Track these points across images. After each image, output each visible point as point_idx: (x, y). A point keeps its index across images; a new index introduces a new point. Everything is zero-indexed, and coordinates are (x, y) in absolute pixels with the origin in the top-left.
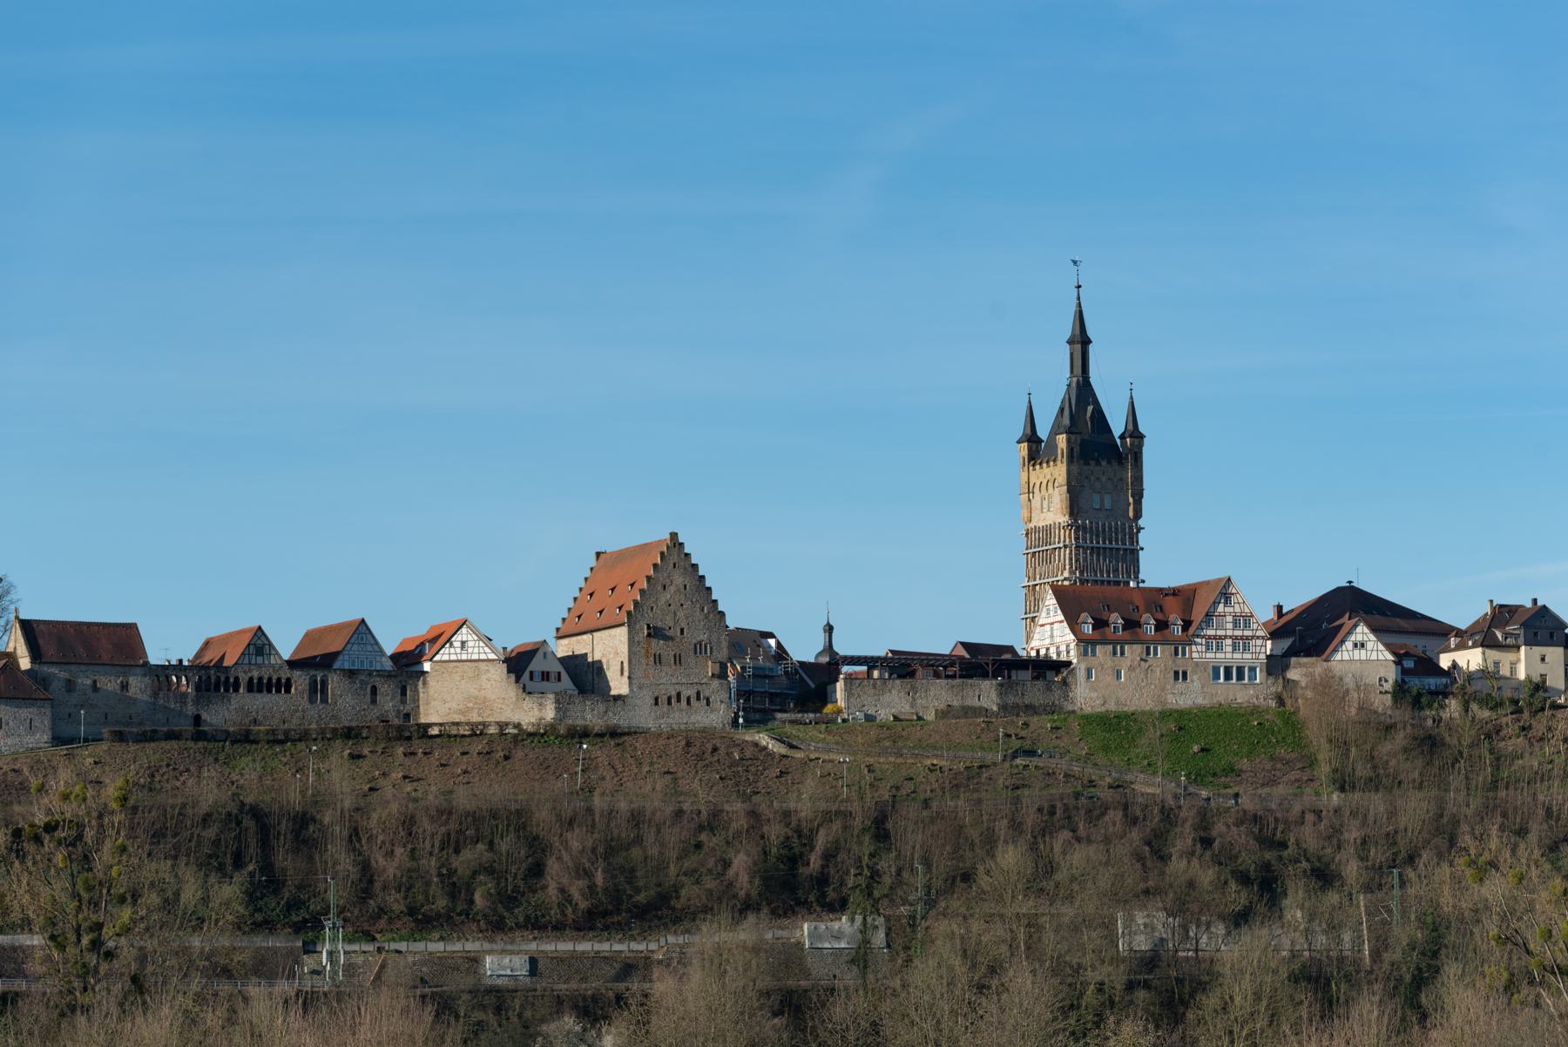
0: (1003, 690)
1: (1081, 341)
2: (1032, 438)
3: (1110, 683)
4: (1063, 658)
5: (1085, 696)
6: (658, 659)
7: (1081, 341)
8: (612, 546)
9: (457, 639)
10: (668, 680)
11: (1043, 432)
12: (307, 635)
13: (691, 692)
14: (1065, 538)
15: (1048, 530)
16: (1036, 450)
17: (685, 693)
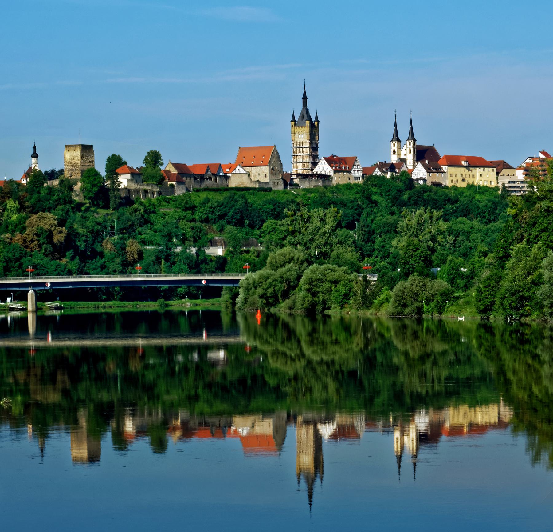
0: (323, 181)
1: (305, 99)
2: (294, 120)
3: (339, 179)
4: (327, 173)
5: (334, 183)
6: (273, 174)
7: (305, 99)
8: (241, 147)
9: (237, 168)
10: (275, 179)
11: (297, 119)
12: (185, 164)
13: (278, 181)
14: (308, 145)
15: (302, 143)
16: (296, 123)
17: (278, 181)
